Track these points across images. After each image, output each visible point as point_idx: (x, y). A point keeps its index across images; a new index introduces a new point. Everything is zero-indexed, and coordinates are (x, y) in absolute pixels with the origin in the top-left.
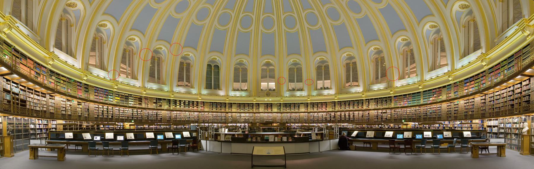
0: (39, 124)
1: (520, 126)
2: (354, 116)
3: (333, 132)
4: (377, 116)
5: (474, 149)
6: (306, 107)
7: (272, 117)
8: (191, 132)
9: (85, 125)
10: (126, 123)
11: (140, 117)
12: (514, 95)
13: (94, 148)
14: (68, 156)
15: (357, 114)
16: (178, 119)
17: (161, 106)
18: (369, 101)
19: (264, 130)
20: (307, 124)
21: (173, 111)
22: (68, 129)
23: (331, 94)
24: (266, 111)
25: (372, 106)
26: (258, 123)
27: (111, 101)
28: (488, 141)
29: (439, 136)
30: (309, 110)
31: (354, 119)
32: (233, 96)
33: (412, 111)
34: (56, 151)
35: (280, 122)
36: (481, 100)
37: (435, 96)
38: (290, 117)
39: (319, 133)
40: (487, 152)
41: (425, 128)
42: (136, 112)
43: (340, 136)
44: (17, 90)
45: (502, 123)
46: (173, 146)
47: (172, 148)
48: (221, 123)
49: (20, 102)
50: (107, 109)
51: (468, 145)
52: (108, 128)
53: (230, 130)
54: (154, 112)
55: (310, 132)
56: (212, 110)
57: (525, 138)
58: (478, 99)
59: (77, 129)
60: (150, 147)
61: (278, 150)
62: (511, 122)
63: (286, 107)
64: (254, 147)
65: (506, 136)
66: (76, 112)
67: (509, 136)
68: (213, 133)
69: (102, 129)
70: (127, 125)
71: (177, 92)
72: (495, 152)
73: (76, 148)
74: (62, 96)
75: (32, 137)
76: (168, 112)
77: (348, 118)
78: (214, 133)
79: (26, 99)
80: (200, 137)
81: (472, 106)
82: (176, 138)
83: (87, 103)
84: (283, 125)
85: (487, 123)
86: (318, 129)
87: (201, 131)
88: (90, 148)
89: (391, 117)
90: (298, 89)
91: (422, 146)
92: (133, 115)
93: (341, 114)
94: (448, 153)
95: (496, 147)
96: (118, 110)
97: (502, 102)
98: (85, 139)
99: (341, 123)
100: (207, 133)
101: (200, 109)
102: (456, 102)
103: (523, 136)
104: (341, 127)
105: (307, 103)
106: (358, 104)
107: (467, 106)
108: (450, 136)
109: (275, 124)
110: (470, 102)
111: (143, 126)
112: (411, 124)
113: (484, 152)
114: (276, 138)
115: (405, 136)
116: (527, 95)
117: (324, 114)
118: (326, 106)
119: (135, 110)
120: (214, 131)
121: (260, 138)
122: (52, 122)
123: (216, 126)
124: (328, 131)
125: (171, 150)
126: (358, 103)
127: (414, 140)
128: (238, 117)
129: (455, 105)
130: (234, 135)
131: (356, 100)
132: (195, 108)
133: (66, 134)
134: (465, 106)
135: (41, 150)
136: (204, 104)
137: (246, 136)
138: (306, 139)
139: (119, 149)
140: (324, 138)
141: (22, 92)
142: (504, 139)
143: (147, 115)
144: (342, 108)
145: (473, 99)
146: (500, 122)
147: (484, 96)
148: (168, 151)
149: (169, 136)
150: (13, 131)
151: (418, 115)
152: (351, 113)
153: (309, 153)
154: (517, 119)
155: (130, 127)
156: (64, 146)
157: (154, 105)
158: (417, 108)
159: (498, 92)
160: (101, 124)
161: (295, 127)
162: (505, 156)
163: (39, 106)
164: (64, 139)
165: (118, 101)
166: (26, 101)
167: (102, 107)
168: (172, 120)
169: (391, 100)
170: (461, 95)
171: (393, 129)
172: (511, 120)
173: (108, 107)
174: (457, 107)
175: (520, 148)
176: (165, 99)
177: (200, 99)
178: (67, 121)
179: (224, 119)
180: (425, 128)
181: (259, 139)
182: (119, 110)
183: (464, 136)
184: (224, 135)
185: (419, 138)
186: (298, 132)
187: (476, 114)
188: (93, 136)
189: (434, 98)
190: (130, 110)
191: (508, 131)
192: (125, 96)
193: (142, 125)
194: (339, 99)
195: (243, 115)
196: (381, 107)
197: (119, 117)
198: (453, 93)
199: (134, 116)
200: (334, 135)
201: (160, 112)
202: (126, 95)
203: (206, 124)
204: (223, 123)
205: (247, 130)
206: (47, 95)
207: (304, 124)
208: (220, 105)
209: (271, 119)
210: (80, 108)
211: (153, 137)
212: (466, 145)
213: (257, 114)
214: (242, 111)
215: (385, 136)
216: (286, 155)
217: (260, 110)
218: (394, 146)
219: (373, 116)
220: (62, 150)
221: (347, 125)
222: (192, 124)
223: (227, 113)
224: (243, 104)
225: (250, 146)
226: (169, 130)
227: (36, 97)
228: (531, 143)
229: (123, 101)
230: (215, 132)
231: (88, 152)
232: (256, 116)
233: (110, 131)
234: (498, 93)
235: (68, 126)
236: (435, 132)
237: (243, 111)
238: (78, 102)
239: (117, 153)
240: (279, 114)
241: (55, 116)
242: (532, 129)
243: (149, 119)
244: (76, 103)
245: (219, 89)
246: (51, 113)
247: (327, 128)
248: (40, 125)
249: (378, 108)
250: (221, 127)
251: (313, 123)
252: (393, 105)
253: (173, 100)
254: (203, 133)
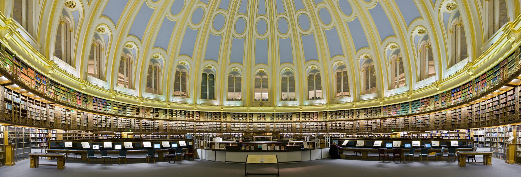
0: (40, 134)
1: (505, 135)
2: (344, 125)
3: (325, 141)
4: (367, 126)
5: (461, 158)
6: (298, 117)
7: (265, 127)
8: (187, 141)
9: (84, 134)
10: (124, 133)
11: (138, 126)
12: (499, 105)
13: (93, 157)
14: (67, 165)
15: (348, 124)
16: (174, 129)
17: (158, 115)
18: (359, 111)
19: (258, 139)
20: (300, 134)
21: (169, 120)
22: (68, 138)
23: (323, 104)
24: (260, 121)
25: (362, 116)
26: (252, 132)
27: (109, 111)
28: (474, 150)
29: (427, 145)
30: (301, 120)
31: (345, 128)
32: (228, 105)
33: (401, 121)
34: (56, 160)
35: (273, 131)
36: (468, 110)
37: (423, 106)
38: (282, 127)
39: (311, 142)
40: (474, 161)
41: (413, 137)
42: (133, 122)
43: (331, 145)
44: (18, 100)
45: (488, 133)
46: (170, 155)
47: (169, 157)
48: (216, 132)
49: (21, 112)
50: (106, 119)
51: (455, 154)
52: (106, 137)
53: (224, 139)
54: (151, 121)
55: (302, 142)
56: (207, 120)
57: (510, 147)
58: (465, 109)
59: (76, 138)
60: (147, 156)
61: (272, 159)
62: (497, 131)
63: (279, 117)
64: (247, 156)
65: (492, 145)
66: (76, 121)
67: (495, 145)
68: (208, 142)
69: (100, 138)
70: (125, 135)
71: (173, 102)
72: (482, 160)
73: (76, 157)
74: (62, 106)
75: (33, 146)
76: (165, 122)
77: (339, 127)
78: (209, 142)
79: (27, 109)
80: (196, 146)
82: (173, 147)
83: (86, 113)
84: (276, 134)
85: (474, 132)
86: (310, 138)
87: (197, 140)
88: (89, 157)
89: (380, 127)
90: (291, 99)
91: (411, 154)
92: (130, 125)
93: (332, 124)
94: (436, 162)
95: (482, 156)
96: (116, 120)
97: (488, 112)
98: (84, 147)
99: (332, 132)
100: (203, 142)
101: (196, 118)
102: (444, 112)
103: (509, 145)
104: (332, 136)
105: (300, 113)
106: (349, 114)
107: (454, 116)
108: (438, 145)
109: (268, 134)
110: (457, 112)
111: (140, 135)
112: (400, 134)
113: (471, 161)
114: (269, 146)
115: (394, 145)
116: (512, 105)
117: (316, 123)
118: (318, 116)
119: (133, 120)
120: (209, 140)
121: (253, 147)
122: (52, 131)
123: (211, 136)
124: (319, 140)
125: (168, 158)
126: (349, 113)
127: (403, 149)
128: (232, 127)
129: (442, 115)
130: (228, 144)
131: (346, 110)
132: (191, 118)
133: (66, 143)
135: (41, 158)
136: (199, 114)
137: (240, 145)
138: (298, 148)
139: (117, 157)
140: (316, 147)
141: (22, 102)
142: (490, 148)
143: (144, 125)
144: (333, 118)
146: (486, 132)
147: (470, 106)
148: (165, 159)
149: (166, 145)
150: (14, 140)
151: (407, 125)
152: (341, 122)
153: (301, 161)
154: (502, 129)
155: (128, 136)
156: (63, 154)
157: (151, 115)
158: (406, 118)
159: (484, 103)
160: (100, 134)
161: (287, 136)
162: (491, 165)
163: (39, 116)
164: (64, 148)
165: (116, 111)
166: (27, 111)
167: (100, 117)
168: (168, 129)
169: (380, 110)
170: (449, 105)
171: (383, 138)
172: (497, 130)
173: (106, 116)
174: (444, 117)
175: (505, 157)
176: (162, 109)
177: (195, 109)
178: (67, 131)
179: (218, 128)
180: (413, 137)
181: (252, 147)
182: (117, 120)
183: (452, 145)
184: (219, 144)
185: (407, 147)
186: (290, 141)
187: (463, 124)
188: (91, 145)
189: (422, 108)
190: (127, 120)
191: (494, 140)
192: (123, 106)
193: (139, 135)
194: (330, 109)
195: (237, 124)
196: (371, 117)
197: (117, 126)
198: (440, 103)
199: (132, 126)
200: (325, 144)
201: (157, 122)
202: (124, 105)
203: (201, 134)
204: (218, 132)
205: (241, 139)
206: (47, 105)
207: (296, 133)
208: (215, 115)
209: (264, 128)
210: (79, 118)
211: (150, 146)
212: (454, 154)
213: (251, 124)
214: (236, 121)
215: (374, 145)
216: (279, 163)
217: (254, 119)
218: (383, 154)
219: (363, 126)
220: (62, 159)
221: (338, 134)
222: (188, 134)
223: (222, 122)
224: (237, 114)
225: (245, 154)
226: (165, 140)
227: (36, 107)
228: (516, 152)
229: (121, 111)
230: (210, 141)
231: (87, 160)
232: (250, 125)
233: (108, 140)
234: (484, 103)
235: (68, 135)
236: (424, 141)
237: (237, 121)
238: (77, 112)
239: (115, 161)
240: (272, 124)
241: (55, 125)
242: (517, 138)
243: (146, 128)
244: (76, 113)
245: (214, 99)
246: (51, 122)
247: (319, 137)
248: (41, 135)
249: (368, 118)
250: (216, 136)
251: (305, 132)
252: (382, 115)
253: (170, 110)
254: (198, 142)
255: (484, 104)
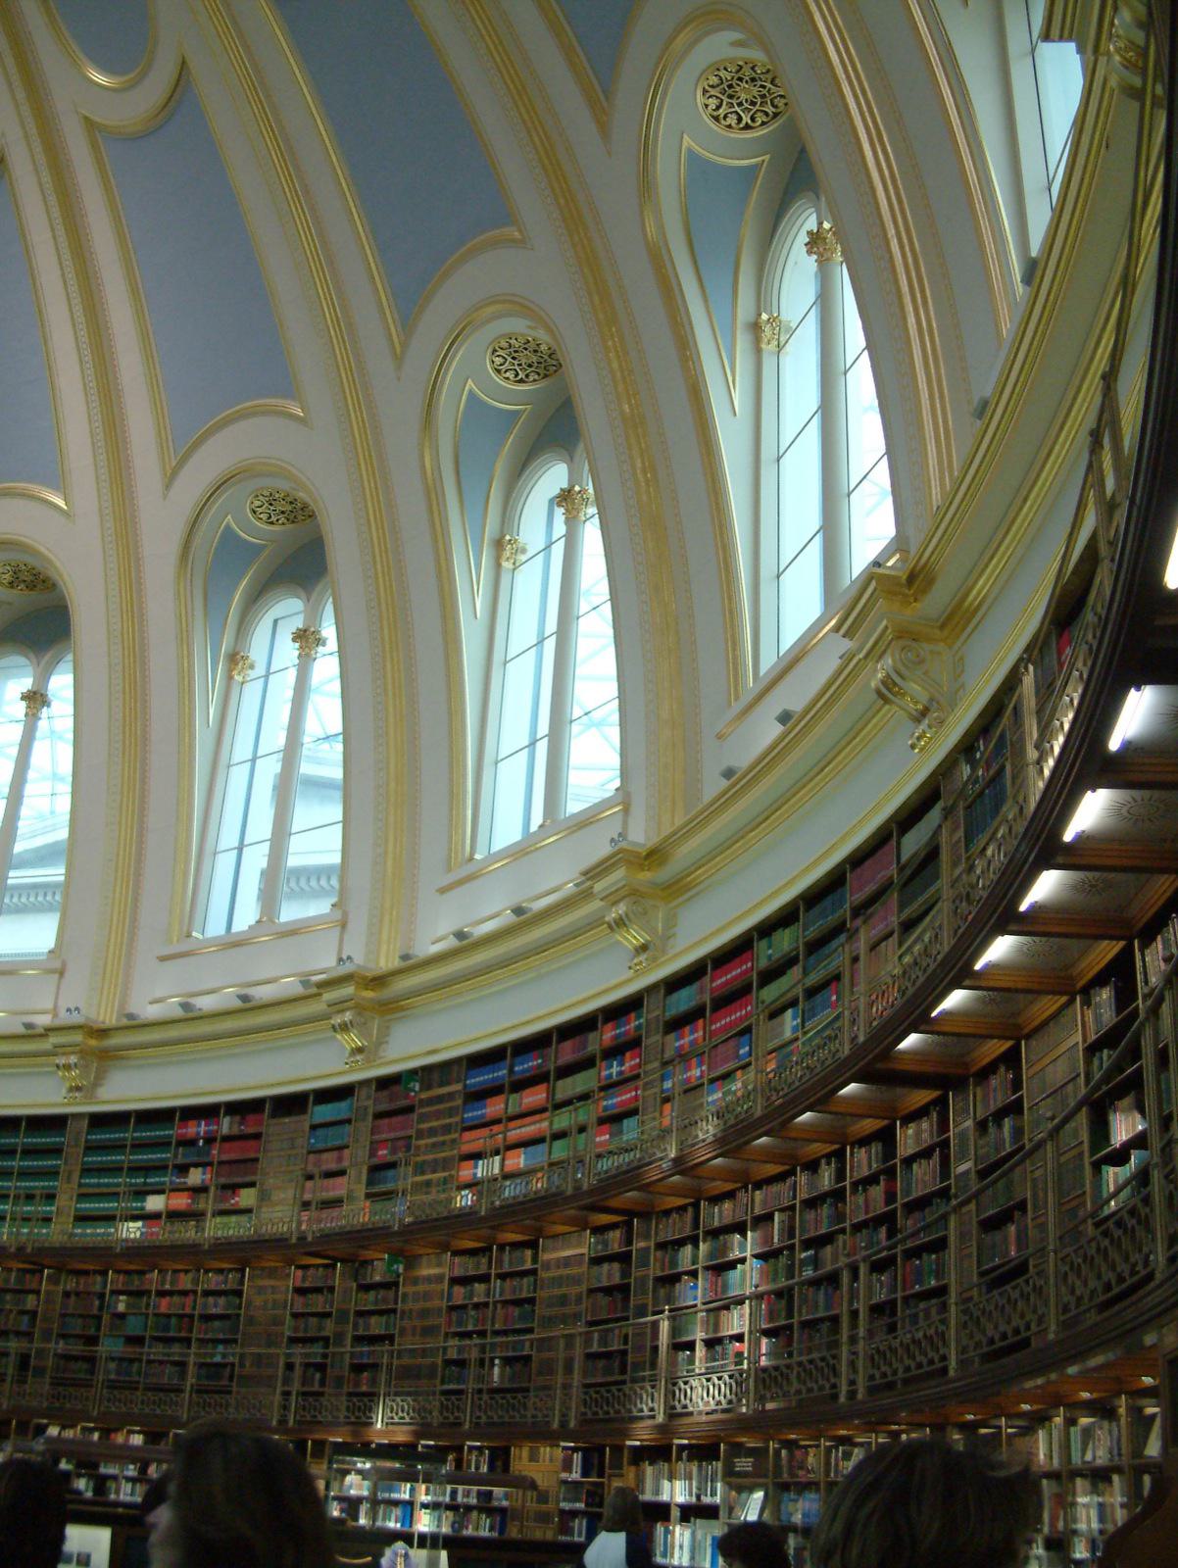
37: (195, 1177)
81: (516, 1311)
107: (477, 1306)
129: (366, 1288)
134: (452, 1308)
145: (529, 1253)
147: (613, 1226)
174: (381, 1313)
255: (728, 1220)
